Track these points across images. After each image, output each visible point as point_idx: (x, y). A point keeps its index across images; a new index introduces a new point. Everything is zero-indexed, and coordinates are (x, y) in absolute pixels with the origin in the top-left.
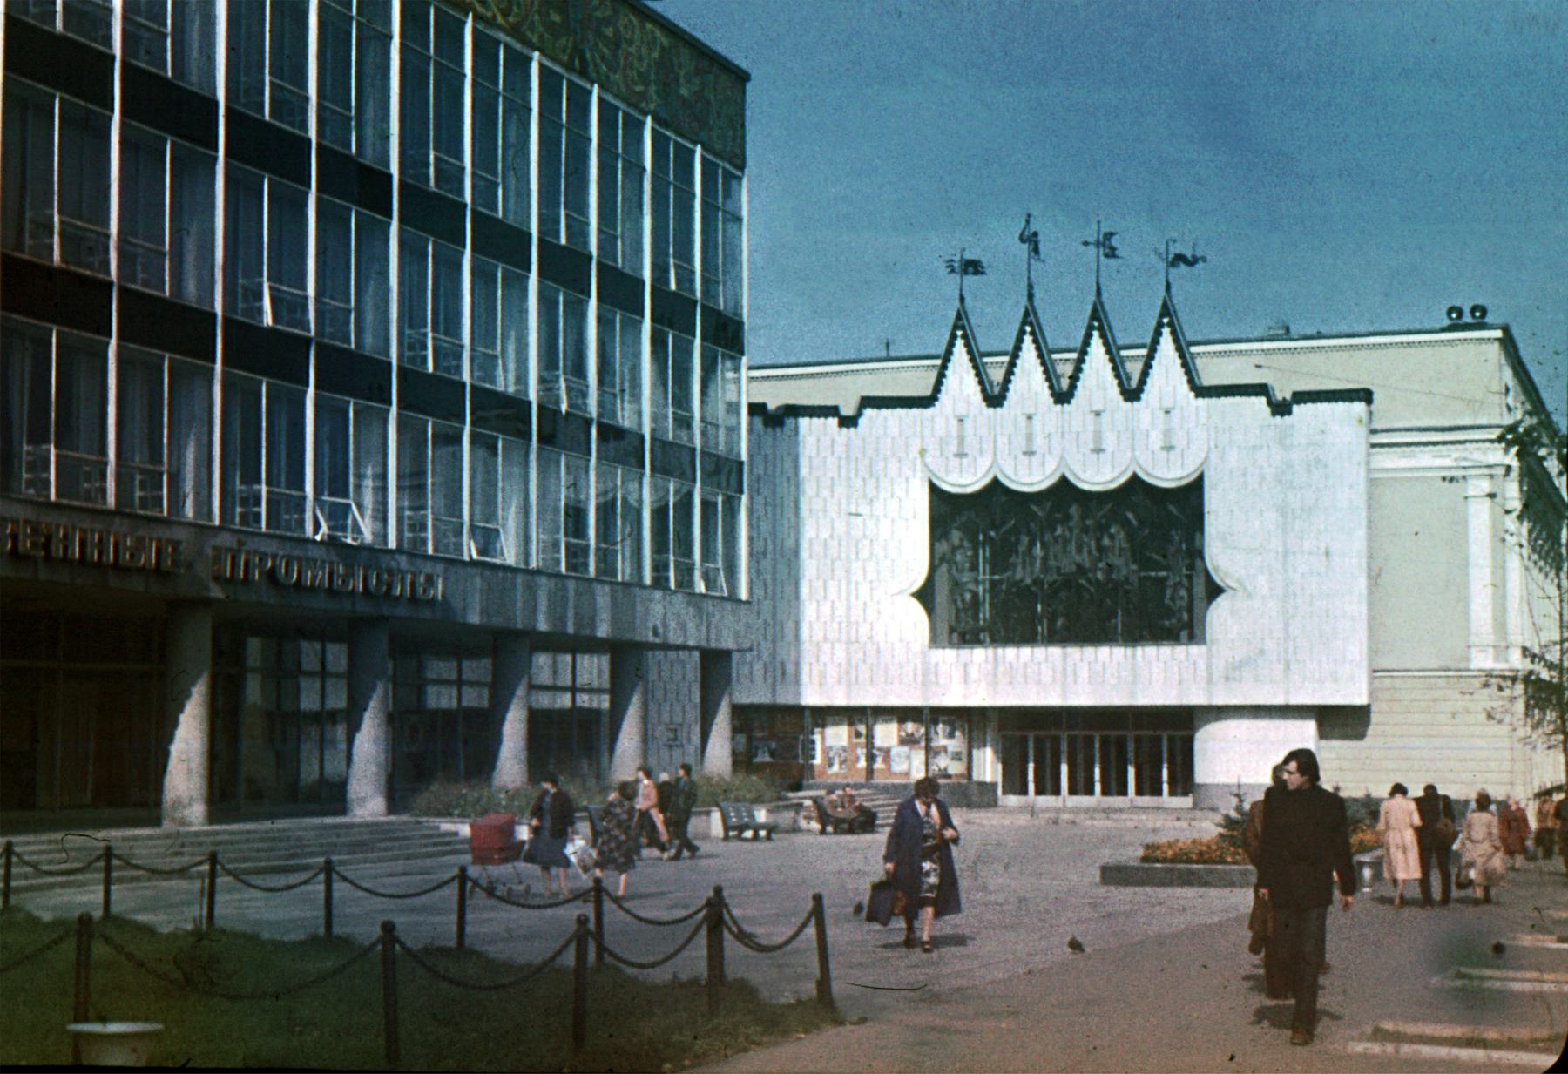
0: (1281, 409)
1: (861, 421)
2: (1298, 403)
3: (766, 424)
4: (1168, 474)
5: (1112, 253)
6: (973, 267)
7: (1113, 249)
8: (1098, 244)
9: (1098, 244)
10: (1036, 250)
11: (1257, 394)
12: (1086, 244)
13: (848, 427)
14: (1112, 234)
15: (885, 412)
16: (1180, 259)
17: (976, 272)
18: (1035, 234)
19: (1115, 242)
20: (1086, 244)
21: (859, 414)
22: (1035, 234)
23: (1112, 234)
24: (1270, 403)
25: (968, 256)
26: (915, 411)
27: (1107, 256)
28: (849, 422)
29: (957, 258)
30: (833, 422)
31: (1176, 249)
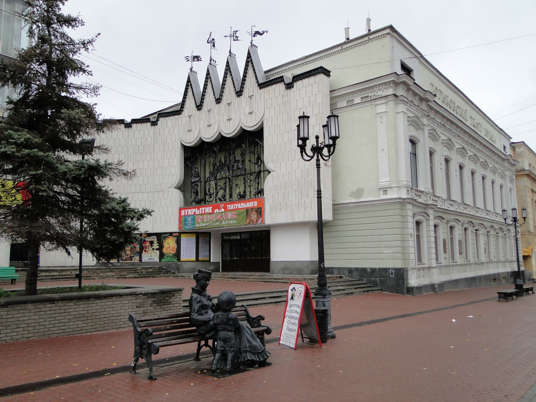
0: (289, 86)
1: (159, 123)
2: (296, 81)
3: (125, 127)
4: (250, 125)
5: (236, 39)
6: (197, 58)
7: (237, 37)
8: (231, 36)
9: (231, 36)
10: (214, 46)
11: (280, 82)
12: (226, 36)
13: (154, 125)
14: (237, 31)
15: (167, 118)
16: (257, 33)
17: (198, 60)
18: (213, 39)
19: (237, 34)
20: (226, 36)
21: (158, 120)
22: (213, 39)
23: (237, 31)
24: (285, 84)
25: (195, 54)
26: (176, 117)
27: (234, 40)
28: (154, 124)
29: (190, 56)
30: (149, 124)
31: (255, 30)
